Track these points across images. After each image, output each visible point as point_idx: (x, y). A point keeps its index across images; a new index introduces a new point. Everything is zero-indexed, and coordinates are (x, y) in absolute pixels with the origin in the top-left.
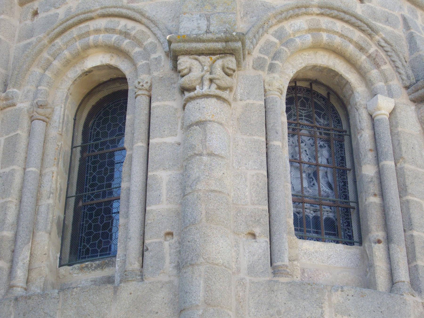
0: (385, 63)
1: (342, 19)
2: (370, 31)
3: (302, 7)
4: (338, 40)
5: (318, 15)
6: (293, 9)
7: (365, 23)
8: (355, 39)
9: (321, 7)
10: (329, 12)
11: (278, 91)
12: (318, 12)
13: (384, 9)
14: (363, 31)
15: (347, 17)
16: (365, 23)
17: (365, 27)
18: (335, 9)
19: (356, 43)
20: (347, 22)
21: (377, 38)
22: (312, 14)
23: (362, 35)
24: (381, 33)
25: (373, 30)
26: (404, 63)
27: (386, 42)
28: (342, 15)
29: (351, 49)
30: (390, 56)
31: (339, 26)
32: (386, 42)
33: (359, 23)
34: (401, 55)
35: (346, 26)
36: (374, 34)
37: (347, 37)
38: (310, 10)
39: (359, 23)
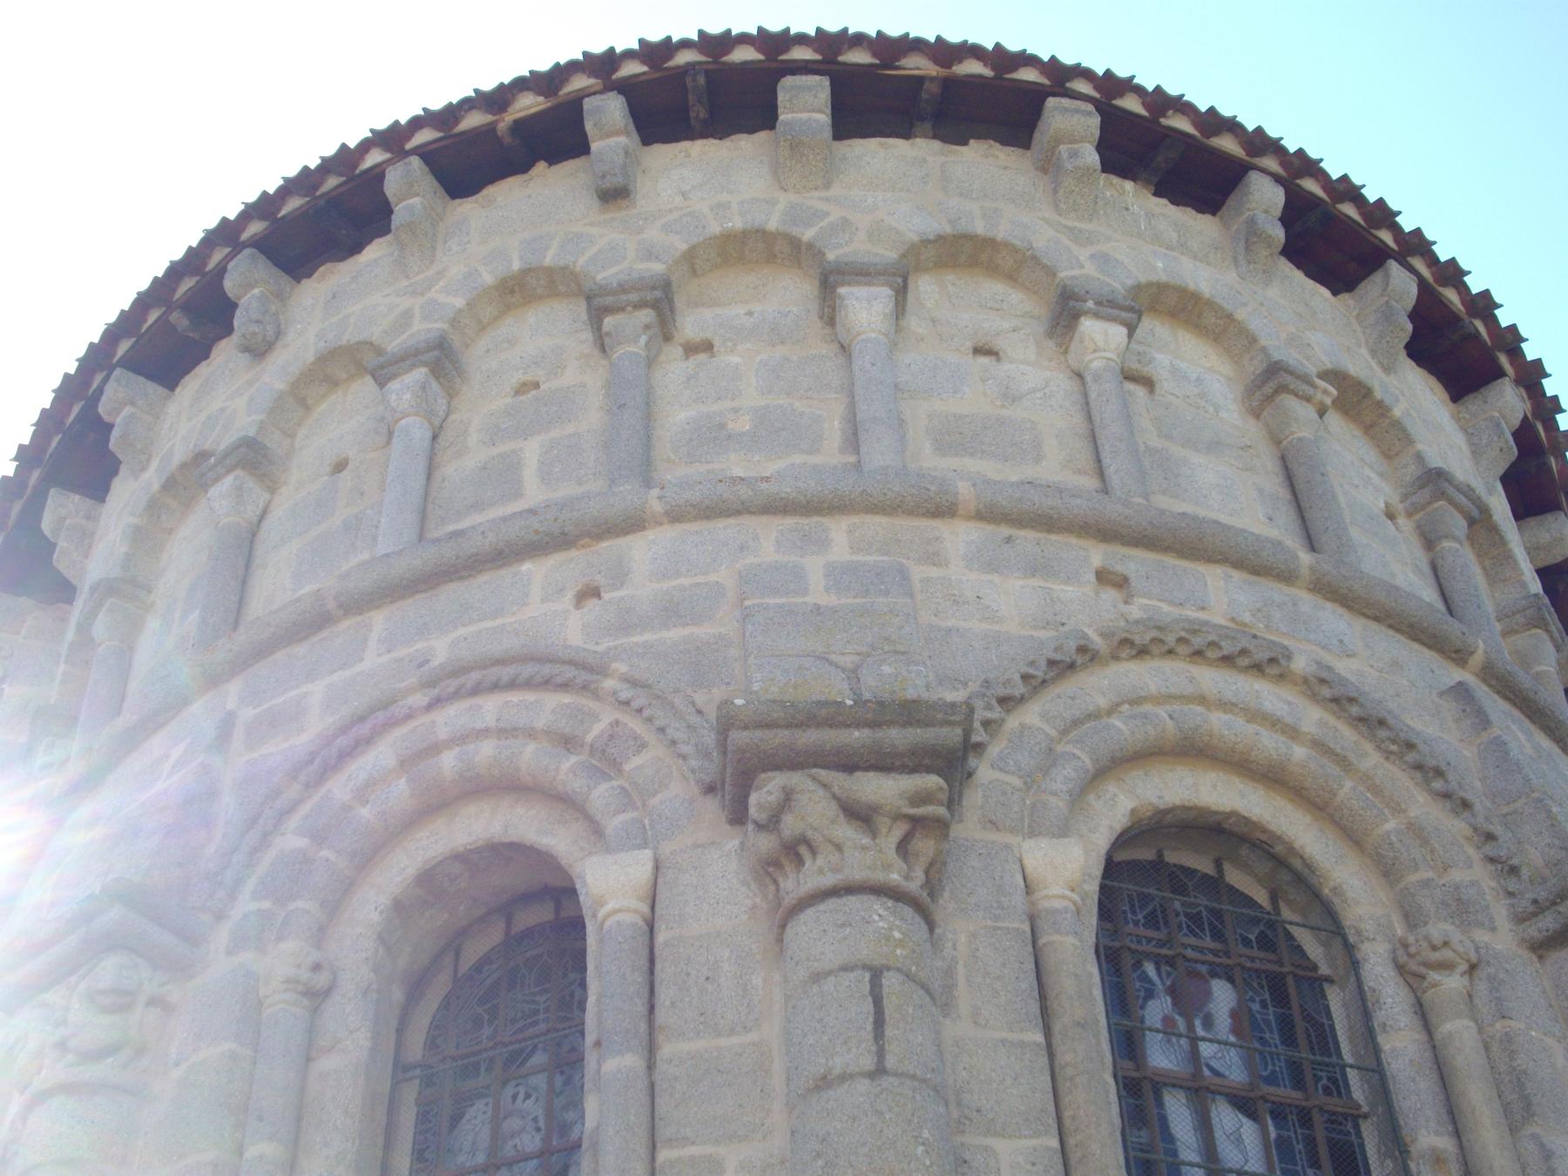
0: (642, 746)
1: (496, 687)
2: (583, 676)
3: (373, 710)
4: (486, 750)
5: (429, 707)
6: (344, 730)
7: (564, 662)
8: (540, 724)
9: (429, 684)
10: (453, 684)
11: (286, 991)
12: (425, 701)
13: (666, 585)
14: (565, 686)
15: (506, 673)
16: (564, 662)
17: (569, 672)
18: (472, 669)
19: (547, 732)
20: (513, 685)
21: (609, 684)
22: (409, 717)
23: (566, 699)
24: (615, 665)
25: (591, 669)
26: (695, 719)
27: (634, 683)
28: (494, 673)
29: (530, 757)
30: (650, 720)
31: (490, 708)
32: (634, 683)
33: (547, 670)
34: (677, 701)
35: (514, 697)
36: (595, 677)
37: (516, 729)
38: (398, 710)
39: (547, 670)
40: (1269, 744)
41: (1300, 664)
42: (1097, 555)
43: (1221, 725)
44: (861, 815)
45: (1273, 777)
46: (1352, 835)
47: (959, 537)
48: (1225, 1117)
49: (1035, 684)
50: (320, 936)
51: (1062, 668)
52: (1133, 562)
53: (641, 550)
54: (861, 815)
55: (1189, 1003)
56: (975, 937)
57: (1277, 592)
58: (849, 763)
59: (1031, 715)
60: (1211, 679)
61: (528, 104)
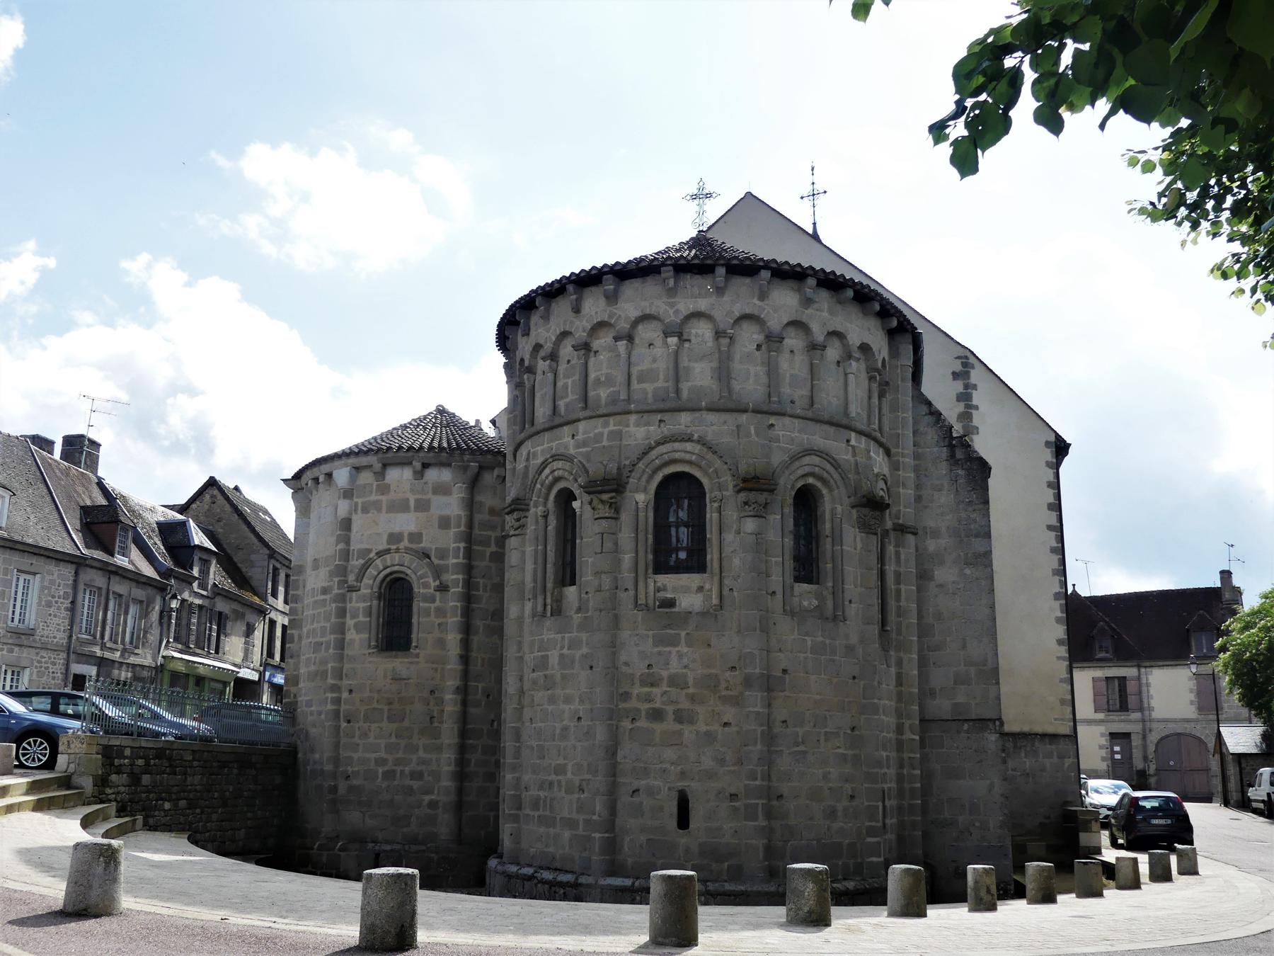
40: (687, 457)
41: (696, 437)
42: (659, 417)
43: (677, 455)
44: (602, 502)
45: (690, 463)
46: (706, 473)
47: (633, 418)
48: (683, 530)
49: (639, 459)
50: (545, 505)
51: (645, 454)
52: (666, 417)
53: (581, 426)
54: (602, 502)
55: (679, 506)
56: (626, 517)
57: (697, 415)
58: (601, 492)
59: (640, 465)
60: (677, 445)
61: (557, 285)
